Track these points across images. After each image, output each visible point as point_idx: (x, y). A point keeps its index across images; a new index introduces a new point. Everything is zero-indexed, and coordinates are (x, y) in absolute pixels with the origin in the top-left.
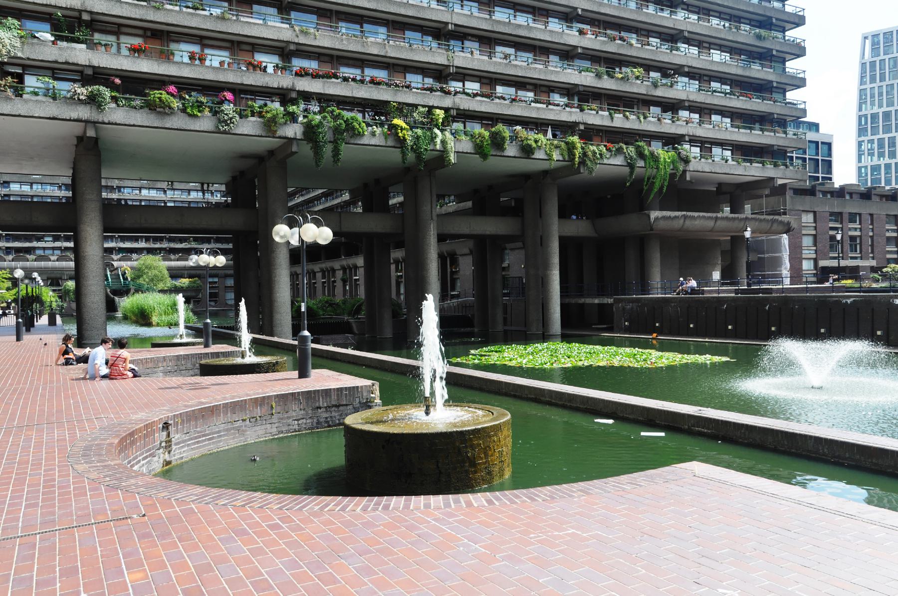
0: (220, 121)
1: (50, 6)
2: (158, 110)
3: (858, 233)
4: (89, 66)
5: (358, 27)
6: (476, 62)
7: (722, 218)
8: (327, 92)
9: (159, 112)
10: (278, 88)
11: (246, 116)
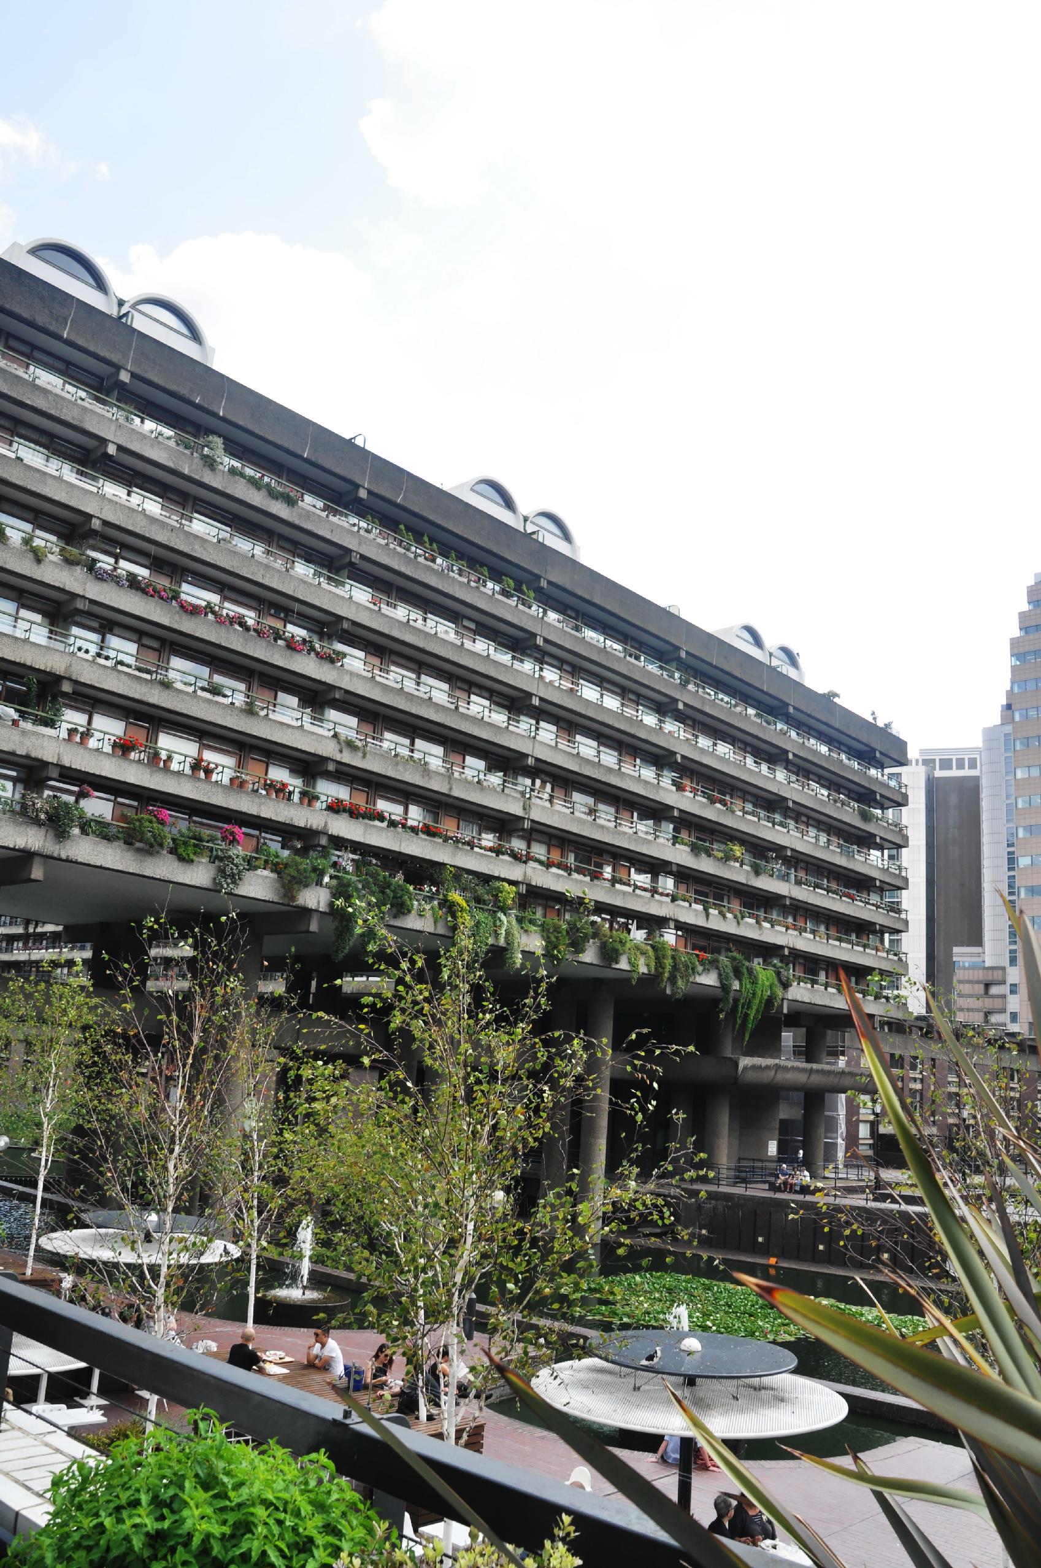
0: (222, 871)
1: (24, 666)
2: (138, 845)
3: (918, 1086)
4: (57, 765)
5: (407, 742)
6: (556, 818)
7: (818, 1071)
8: (368, 842)
9: (139, 850)
10: (304, 829)
11: (256, 868)
